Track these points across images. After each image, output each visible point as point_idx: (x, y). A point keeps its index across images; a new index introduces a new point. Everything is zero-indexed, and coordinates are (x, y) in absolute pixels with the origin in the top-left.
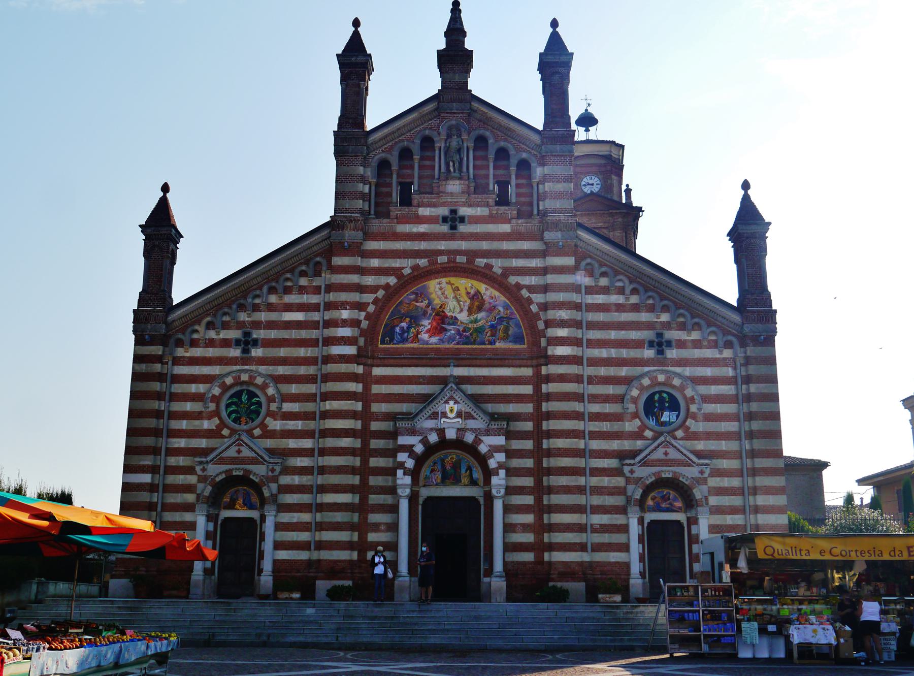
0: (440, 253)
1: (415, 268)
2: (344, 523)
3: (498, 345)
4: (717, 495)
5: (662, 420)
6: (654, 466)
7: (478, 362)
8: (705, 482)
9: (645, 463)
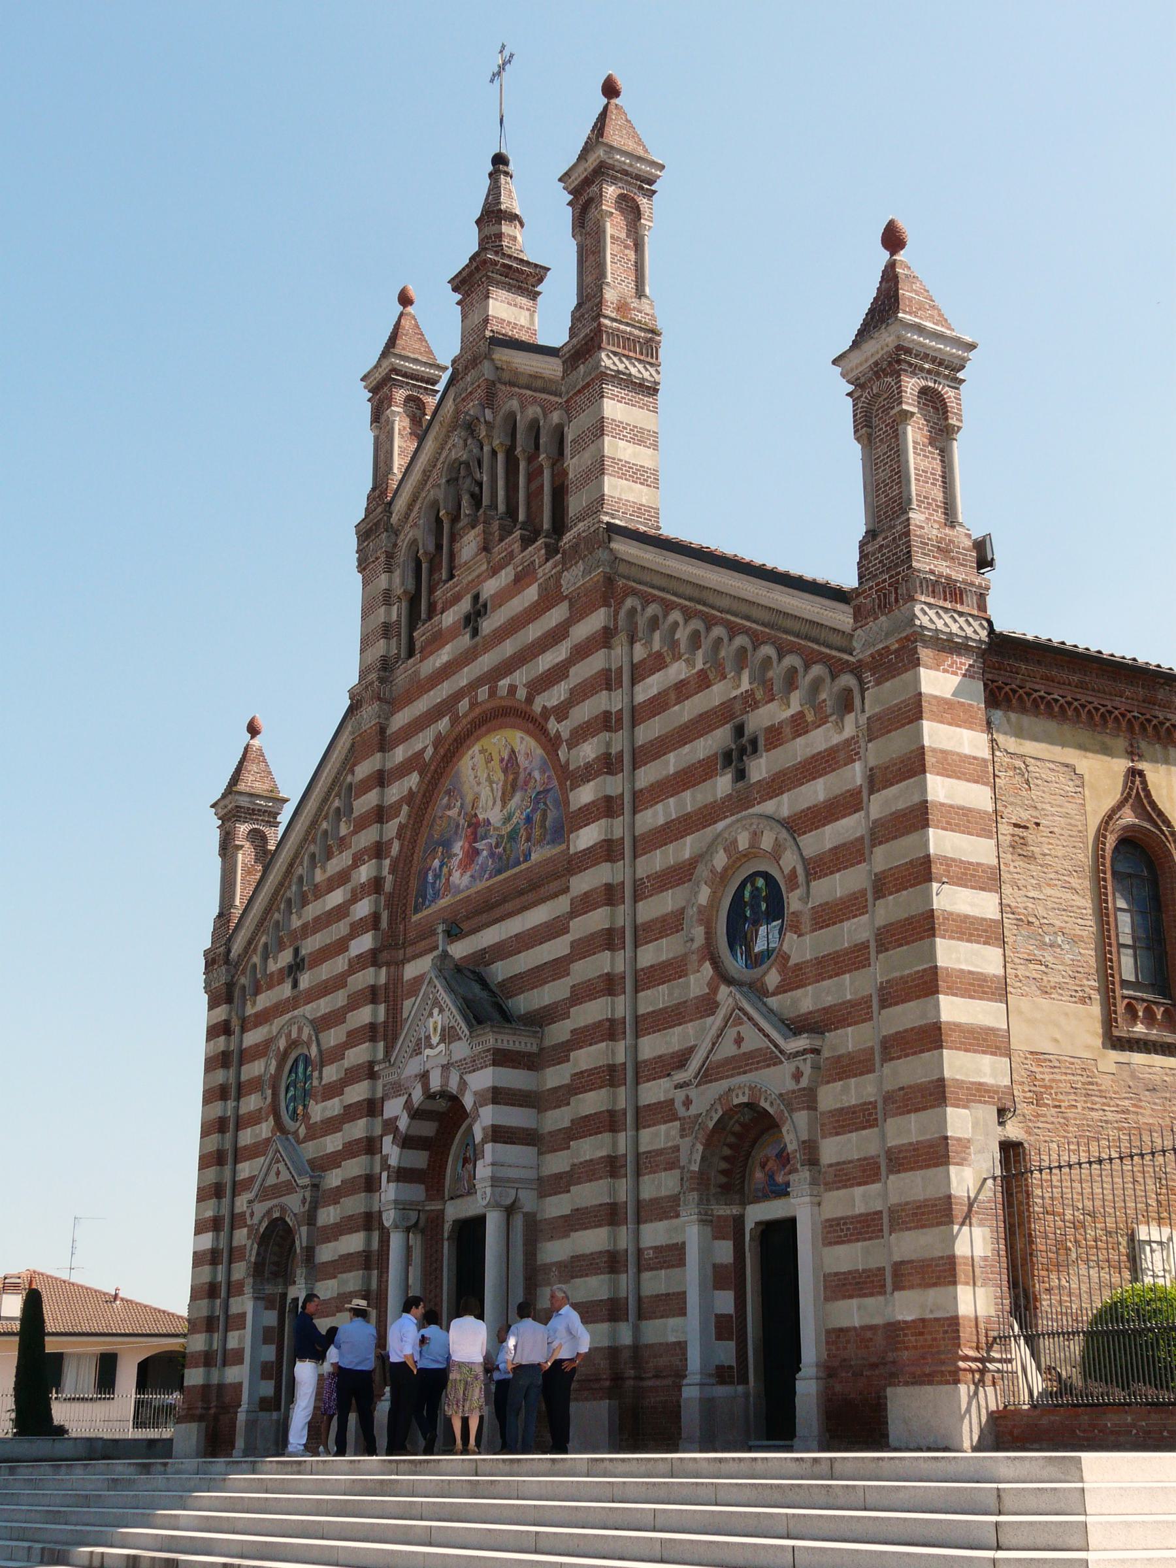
0: (457, 696)
1: (438, 741)
2: (354, 1292)
3: (534, 856)
4: (837, 1134)
5: (757, 950)
6: (716, 1080)
7: (509, 906)
8: (809, 1099)
9: (707, 1075)
